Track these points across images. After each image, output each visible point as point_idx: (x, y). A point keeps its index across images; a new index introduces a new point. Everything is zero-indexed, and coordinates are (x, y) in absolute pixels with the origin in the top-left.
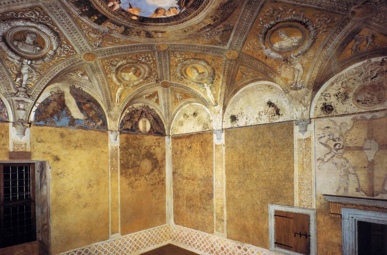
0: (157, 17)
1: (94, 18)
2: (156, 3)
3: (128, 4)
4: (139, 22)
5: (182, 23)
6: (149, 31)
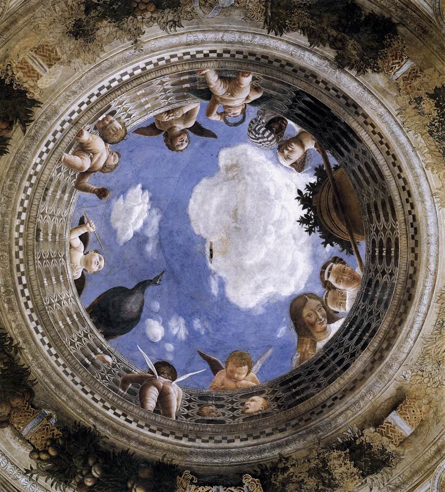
0: (320, 345)
2: (269, 289)
3: (198, 356)
4: (282, 416)
5: (410, 298)
6: (349, 434)
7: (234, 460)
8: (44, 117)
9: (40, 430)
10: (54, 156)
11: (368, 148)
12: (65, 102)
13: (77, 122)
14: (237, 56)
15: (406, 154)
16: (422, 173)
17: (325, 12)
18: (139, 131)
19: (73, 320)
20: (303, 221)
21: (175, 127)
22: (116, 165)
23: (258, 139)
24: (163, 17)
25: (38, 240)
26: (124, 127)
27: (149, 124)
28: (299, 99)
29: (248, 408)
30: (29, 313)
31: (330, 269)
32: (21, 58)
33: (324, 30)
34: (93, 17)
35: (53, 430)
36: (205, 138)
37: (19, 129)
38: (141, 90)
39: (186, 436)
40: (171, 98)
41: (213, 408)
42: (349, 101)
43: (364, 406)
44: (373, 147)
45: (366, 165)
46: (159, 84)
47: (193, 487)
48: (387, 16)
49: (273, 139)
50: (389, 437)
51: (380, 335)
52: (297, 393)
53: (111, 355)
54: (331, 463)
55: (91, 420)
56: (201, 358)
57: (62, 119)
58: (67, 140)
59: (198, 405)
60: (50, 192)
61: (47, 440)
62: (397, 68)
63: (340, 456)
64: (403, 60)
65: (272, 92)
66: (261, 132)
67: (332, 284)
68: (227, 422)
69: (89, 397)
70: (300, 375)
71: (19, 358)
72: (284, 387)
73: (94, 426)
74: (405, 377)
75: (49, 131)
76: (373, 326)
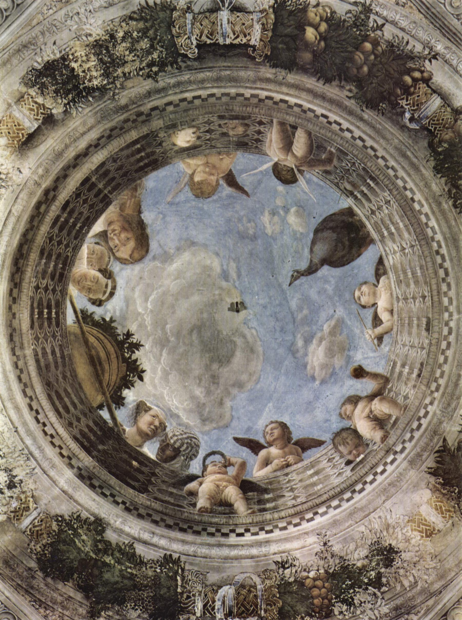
1: (316, 27)
3: (249, 192)
7: (208, 74)
8: (424, 457)
9: (422, 104)
10: (412, 413)
11: (66, 429)
12: (401, 474)
13: (387, 452)
14: (213, 530)
15: (25, 424)
16: (5, 404)
17: (117, 583)
18: (319, 443)
19: (387, 228)
20: (137, 346)
21: (280, 449)
22: (344, 404)
23: (188, 438)
24: (296, 572)
25: (428, 319)
26: (335, 447)
27: (309, 452)
28: (143, 483)
29: (193, 133)
30: (436, 236)
31: (105, 293)
32: (450, 522)
33: (119, 562)
34: (373, 570)
35: (407, 105)
36: (246, 436)
37: (450, 442)
38: (319, 491)
39: (260, 100)
40: (285, 482)
41: (231, 133)
42: (88, 482)
43: (65, 137)
44: (61, 431)
45: (68, 411)
46: (299, 497)
47: (252, 43)
48: (49, 580)
49: (171, 438)
50: (36, 103)
51: (49, 219)
52: (139, 151)
54: (99, 73)
55: (366, 116)
56: (246, 189)
57: (403, 455)
58: (399, 432)
59: (248, 135)
60: (416, 372)
61: (414, 93)
62: (36, 521)
63: (90, 81)
64: (30, 530)
65: (174, 491)
66: (185, 446)
67: (103, 275)
68: (216, 118)
69: (369, 142)
70: (137, 171)
71: (446, 185)
72: (152, 158)
73: (363, 110)
74: (20, 171)
75: (419, 440)
76: (56, 230)
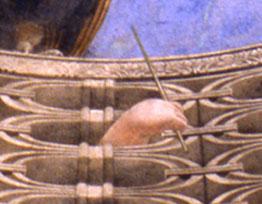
53: (149, 86)
